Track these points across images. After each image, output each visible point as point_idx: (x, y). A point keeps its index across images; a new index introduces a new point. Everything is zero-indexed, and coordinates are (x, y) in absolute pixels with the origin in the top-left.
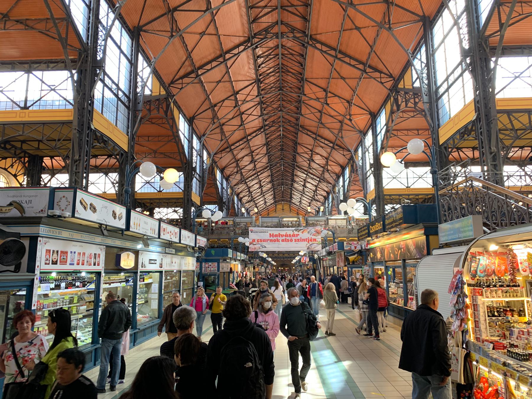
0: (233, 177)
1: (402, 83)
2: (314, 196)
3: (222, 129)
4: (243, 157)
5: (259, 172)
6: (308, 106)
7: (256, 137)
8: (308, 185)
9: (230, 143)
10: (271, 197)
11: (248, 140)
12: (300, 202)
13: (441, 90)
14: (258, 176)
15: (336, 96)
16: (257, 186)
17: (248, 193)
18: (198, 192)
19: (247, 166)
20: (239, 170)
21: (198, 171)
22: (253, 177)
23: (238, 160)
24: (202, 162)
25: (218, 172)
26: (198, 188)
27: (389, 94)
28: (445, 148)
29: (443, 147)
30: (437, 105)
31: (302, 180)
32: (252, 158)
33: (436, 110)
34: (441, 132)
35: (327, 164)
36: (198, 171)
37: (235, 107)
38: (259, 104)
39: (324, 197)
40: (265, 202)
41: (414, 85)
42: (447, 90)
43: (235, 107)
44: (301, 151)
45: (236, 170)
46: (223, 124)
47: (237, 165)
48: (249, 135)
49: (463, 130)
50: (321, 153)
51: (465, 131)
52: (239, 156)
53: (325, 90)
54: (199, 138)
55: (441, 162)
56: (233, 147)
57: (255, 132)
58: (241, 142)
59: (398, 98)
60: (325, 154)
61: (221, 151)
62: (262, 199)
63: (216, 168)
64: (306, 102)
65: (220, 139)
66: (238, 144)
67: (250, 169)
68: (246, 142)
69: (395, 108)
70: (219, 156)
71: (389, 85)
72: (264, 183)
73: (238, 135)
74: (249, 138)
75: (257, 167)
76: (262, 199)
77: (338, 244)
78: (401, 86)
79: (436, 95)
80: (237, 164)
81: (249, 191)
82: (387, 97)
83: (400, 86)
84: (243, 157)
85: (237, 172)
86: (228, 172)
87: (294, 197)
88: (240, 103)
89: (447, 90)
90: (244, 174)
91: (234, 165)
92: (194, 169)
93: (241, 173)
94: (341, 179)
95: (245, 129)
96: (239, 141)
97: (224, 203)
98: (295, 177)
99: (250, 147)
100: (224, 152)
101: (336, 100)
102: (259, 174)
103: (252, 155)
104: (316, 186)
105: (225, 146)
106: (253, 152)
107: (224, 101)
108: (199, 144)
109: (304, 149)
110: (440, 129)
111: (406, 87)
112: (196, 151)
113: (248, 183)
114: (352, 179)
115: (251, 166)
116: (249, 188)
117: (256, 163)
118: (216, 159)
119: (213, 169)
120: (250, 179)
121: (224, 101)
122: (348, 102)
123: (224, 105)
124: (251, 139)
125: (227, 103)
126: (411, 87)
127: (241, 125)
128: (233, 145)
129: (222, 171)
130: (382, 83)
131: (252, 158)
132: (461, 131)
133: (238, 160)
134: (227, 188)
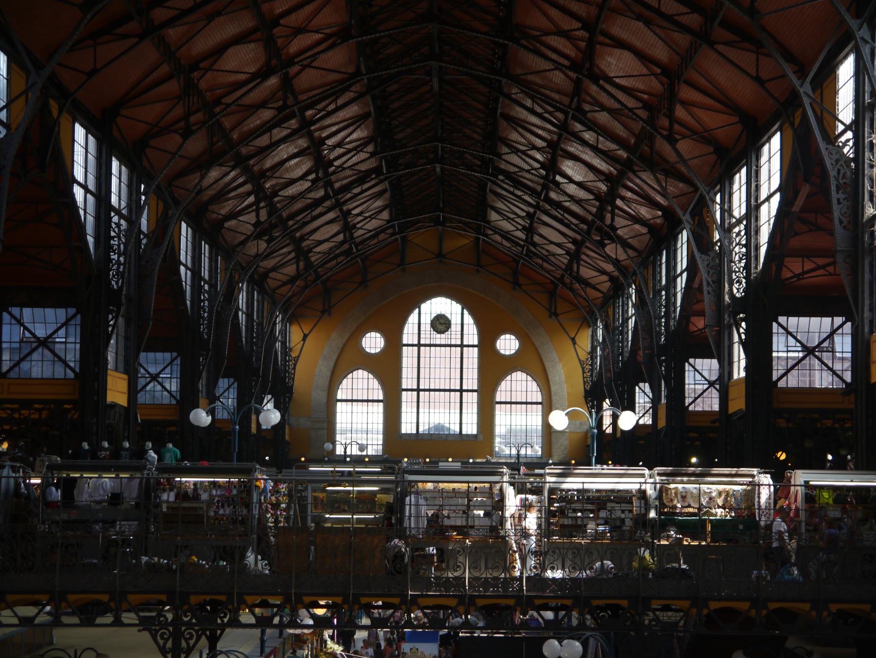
2: (600, 215)
4: (221, 49)
8: (569, 167)
10: (379, 203)
12: (530, 230)
16: (300, 167)
17: (252, 199)
23: (194, 66)
25: (80, 132)
31: (540, 143)
35: (671, 97)
39: (652, 229)
40: (348, 228)
44: (542, 22)
50: (638, 44)
60: (660, 52)
62: (331, 215)
63: (65, 119)
76: (331, 215)
81: (258, 191)
84: (221, 49)
87: (499, 205)
91: (173, 86)
94: (740, 179)
97: (114, 297)
98: (503, 123)
104: (607, 177)
106: (275, 21)
109: (554, 12)
114: (796, 208)
134: (134, 208)
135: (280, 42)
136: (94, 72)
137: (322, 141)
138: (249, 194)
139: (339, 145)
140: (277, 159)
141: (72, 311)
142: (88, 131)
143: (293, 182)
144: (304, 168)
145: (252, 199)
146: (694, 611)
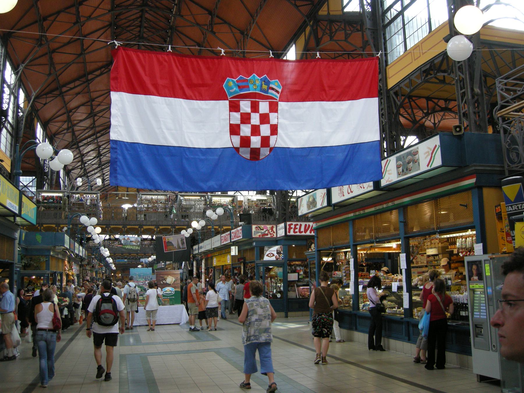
0: (60, 136)
1: (325, 8)
3: (51, 58)
4: (78, 107)
5: (99, 132)
6: (182, 36)
7: (98, 79)
9: (61, 82)
11: (88, 80)
13: (393, 12)
14: (97, 138)
15: (225, 22)
16: (93, 154)
17: (79, 164)
18: (8, 154)
19: (81, 121)
20: (71, 126)
21: (10, 119)
22: (89, 140)
24: (17, 106)
26: (9, 146)
27: (305, 22)
28: (396, 94)
29: (392, 92)
30: (384, 34)
32: (92, 109)
33: (383, 41)
34: (390, 72)
36: (10, 119)
37: (75, 24)
38: (110, 25)
41: (346, 10)
42: (401, 13)
43: (75, 24)
45: (65, 126)
46: (54, 51)
47: (69, 120)
48: (91, 72)
49: (428, 66)
51: (431, 66)
52: (73, 104)
53: (210, 13)
54: (15, 68)
55: (389, 113)
56: (64, 89)
57: (100, 68)
58: (77, 83)
59: (317, 29)
61: (46, 94)
62: (98, 175)
63: (36, 120)
64: (180, 29)
65: (48, 72)
66: (72, 85)
67: (87, 126)
68: (84, 82)
69: (313, 43)
70: (43, 101)
71: (306, 9)
72: (105, 151)
73: (73, 71)
74: (90, 77)
75: (97, 124)
76: (98, 175)
77: (242, 229)
78: (323, 12)
79: (383, 20)
80: (69, 117)
82: (300, 28)
83: (321, 13)
84: (78, 107)
85: (68, 129)
86: (54, 127)
88: (82, 19)
89: (401, 13)
90: (77, 133)
92: (5, 113)
93: (73, 132)
95: (84, 63)
96: (74, 81)
99: (89, 92)
100: (50, 95)
101: (225, 28)
102: (98, 135)
103: (92, 106)
105: (53, 86)
106: (93, 100)
107: (58, 13)
108: (13, 76)
110: (388, 67)
111: (331, 13)
112: (9, 86)
113: (81, 148)
115: (87, 123)
116: (82, 155)
117: (96, 118)
118: (38, 106)
119: (32, 121)
120: (85, 142)
121: (58, 13)
122: (242, 33)
123: (58, 19)
124: (93, 79)
125: (63, 17)
126: (341, 13)
127: (81, 54)
128: (65, 85)
129: (45, 127)
130: (297, 7)
131: (92, 109)
132: (423, 69)
133: (70, 111)
135: (94, 107)
136: (45, 104)
137: (100, 147)
138: (79, 162)
139: (104, 148)
140: (87, 151)
141: (34, 177)
142: (41, 125)
143: (90, 160)
144: (94, 155)
145: (79, 164)
146: (219, 229)
